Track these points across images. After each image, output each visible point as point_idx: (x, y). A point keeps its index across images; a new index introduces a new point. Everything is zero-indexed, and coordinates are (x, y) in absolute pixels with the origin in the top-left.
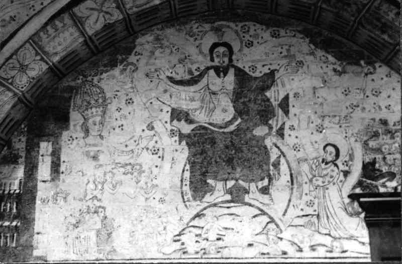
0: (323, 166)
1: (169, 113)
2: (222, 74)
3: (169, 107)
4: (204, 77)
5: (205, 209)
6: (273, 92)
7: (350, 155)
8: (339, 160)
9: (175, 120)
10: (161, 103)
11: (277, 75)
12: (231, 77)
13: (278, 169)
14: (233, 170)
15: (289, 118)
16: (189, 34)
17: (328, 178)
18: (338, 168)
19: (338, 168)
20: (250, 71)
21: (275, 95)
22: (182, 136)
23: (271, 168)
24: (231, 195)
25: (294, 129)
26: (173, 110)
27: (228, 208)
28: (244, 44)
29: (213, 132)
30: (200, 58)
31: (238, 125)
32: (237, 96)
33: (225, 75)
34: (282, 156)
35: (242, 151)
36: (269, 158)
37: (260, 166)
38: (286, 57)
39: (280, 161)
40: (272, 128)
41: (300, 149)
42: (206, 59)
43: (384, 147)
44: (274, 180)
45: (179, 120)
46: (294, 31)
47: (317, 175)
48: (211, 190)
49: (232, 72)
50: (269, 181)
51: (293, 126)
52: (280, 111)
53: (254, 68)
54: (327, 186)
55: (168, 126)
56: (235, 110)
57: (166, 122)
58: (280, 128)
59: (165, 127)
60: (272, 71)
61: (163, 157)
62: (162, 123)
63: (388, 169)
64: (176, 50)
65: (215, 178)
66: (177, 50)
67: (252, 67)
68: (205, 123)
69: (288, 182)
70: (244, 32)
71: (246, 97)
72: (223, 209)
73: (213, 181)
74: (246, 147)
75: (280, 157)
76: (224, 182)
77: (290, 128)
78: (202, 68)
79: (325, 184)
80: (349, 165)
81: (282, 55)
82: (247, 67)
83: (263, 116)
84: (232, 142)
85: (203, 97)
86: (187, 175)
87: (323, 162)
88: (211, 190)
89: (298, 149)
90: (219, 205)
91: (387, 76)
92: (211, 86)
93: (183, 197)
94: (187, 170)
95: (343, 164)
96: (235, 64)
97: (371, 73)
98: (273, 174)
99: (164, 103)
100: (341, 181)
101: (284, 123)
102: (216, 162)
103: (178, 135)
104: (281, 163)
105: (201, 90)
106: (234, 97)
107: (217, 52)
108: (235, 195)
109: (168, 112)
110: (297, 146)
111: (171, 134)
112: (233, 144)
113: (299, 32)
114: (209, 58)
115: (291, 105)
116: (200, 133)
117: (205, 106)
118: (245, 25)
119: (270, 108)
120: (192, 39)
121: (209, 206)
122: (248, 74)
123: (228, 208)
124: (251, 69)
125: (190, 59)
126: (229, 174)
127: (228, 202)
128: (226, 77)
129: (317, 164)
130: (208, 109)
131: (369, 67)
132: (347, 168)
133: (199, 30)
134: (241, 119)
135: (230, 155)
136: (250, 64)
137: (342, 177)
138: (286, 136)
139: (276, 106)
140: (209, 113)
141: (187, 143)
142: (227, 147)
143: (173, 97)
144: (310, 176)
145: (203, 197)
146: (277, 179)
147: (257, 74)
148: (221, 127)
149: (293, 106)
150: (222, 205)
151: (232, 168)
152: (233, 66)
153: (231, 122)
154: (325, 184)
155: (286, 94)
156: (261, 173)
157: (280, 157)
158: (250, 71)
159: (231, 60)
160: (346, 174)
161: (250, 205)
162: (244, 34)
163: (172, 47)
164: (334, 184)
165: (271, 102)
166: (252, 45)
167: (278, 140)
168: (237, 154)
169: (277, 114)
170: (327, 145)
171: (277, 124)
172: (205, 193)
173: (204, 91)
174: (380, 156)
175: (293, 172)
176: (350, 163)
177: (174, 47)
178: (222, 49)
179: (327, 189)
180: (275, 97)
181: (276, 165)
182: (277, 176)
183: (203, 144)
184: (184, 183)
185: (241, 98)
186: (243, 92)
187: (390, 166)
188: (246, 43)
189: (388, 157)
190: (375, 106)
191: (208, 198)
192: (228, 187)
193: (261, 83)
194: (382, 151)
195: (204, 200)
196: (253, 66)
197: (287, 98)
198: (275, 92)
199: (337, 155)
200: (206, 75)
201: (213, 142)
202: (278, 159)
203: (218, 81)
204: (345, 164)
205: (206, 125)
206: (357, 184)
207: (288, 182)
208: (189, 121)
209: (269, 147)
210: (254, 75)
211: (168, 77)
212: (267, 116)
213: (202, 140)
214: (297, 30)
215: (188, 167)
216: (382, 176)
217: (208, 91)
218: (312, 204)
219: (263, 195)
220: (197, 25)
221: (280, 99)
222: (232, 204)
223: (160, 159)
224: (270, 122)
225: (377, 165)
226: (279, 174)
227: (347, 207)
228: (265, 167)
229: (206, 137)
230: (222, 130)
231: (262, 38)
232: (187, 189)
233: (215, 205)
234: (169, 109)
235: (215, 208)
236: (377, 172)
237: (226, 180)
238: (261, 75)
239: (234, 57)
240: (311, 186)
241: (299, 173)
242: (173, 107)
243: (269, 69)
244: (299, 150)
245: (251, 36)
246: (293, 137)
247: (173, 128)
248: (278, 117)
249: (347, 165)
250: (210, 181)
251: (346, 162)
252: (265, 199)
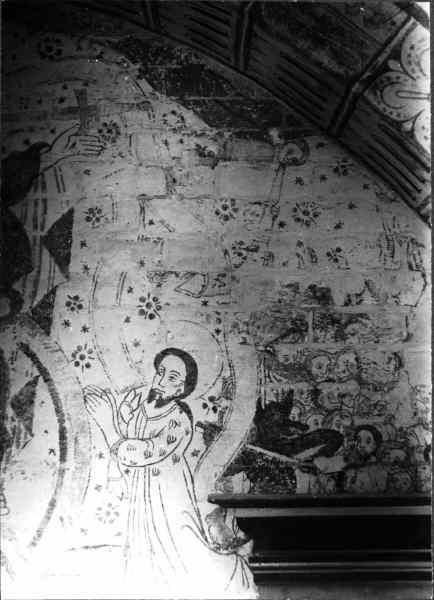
0: (151, 409)
7: (225, 382)
8: (194, 394)
15: (67, 277)
17: (161, 444)
18: (191, 418)
19: (191, 418)
43: (315, 362)
47: (131, 435)
51: (76, 298)
54: (156, 466)
58: (43, 302)
63: (323, 424)
79: (151, 460)
80: (219, 409)
87: (150, 399)
89: (87, 361)
91: (336, 170)
95: (205, 406)
97: (295, 162)
98: (14, 430)
100: (195, 454)
110: (84, 352)
115: (76, 241)
129: (134, 405)
131: (290, 146)
132: (213, 418)
137: (198, 443)
144: (114, 438)
149: (83, 244)
154: (151, 460)
157: (34, 383)
160: (211, 432)
164: (176, 460)
170: (165, 353)
171: (34, 294)
174: (304, 386)
176: (225, 403)
179: (157, 473)
182: (22, 436)
187: (330, 412)
189: (326, 389)
190: (300, 251)
194: (309, 373)
199: (191, 382)
202: (31, 389)
204: (211, 405)
206: (237, 461)
216: (306, 442)
218: (112, 516)
224: (17, 286)
225: (295, 412)
227: (206, 528)
236: (292, 429)
240: (113, 465)
241: (84, 428)
244: (88, 366)
249: (215, 409)
251: (212, 399)
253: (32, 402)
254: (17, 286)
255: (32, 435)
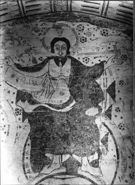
1: (15, 94)
2: (60, 64)
3: (16, 90)
4: (46, 64)
5: (43, 180)
6: (102, 80)
9: (20, 101)
10: (9, 86)
11: (106, 66)
12: (68, 66)
13: (106, 145)
14: (68, 145)
15: (115, 102)
16: (35, 30)
20: (84, 62)
21: (104, 82)
22: (25, 115)
23: (101, 144)
24: (66, 168)
25: (120, 111)
26: (18, 91)
27: (63, 179)
28: (79, 39)
29: (51, 111)
30: (43, 50)
31: (73, 106)
32: (73, 83)
33: (63, 65)
34: (109, 133)
35: (76, 129)
36: (98, 135)
37: (91, 143)
38: (112, 51)
39: (107, 138)
40: (102, 109)
41: (125, 128)
42: (48, 51)
44: (103, 155)
45: (23, 101)
46: (119, 31)
48: (49, 163)
49: (69, 61)
50: (99, 155)
51: (118, 108)
52: (108, 95)
53: (87, 60)
55: (14, 106)
56: (71, 94)
57: (12, 102)
58: (108, 109)
59: (11, 106)
60: (102, 62)
61: (8, 133)
62: (8, 103)
64: (23, 42)
65: (53, 152)
66: (24, 43)
67: (86, 59)
68: (46, 104)
69: (115, 156)
70: (79, 30)
71: (79, 83)
72: (58, 180)
73: (51, 155)
74: (80, 125)
75: (107, 134)
76: (60, 156)
77: (116, 110)
78: (45, 58)
81: (110, 49)
82: (81, 58)
83: (93, 99)
84: (67, 120)
85: (45, 81)
86: (28, 148)
88: (49, 163)
90: (55, 177)
92: (51, 73)
93: (24, 168)
94: (29, 145)
96: (72, 56)
98: (102, 149)
99: (11, 86)
101: (111, 106)
102: (54, 138)
103: (22, 113)
104: (109, 140)
105: (43, 75)
106: (70, 83)
107: (57, 45)
108: (69, 168)
109: (14, 93)
111: (16, 112)
112: (69, 123)
113: (123, 32)
114: (50, 50)
116: (41, 113)
117: (46, 89)
118: (81, 25)
119: (100, 92)
120: (37, 34)
121: (47, 178)
122: (83, 64)
123: (63, 179)
124: (85, 60)
125: (34, 50)
126: (65, 148)
127: (63, 174)
128: (64, 66)
130: (48, 91)
133: (42, 27)
134: (76, 101)
135: (65, 132)
136: (84, 56)
138: (113, 117)
139: (104, 91)
140: (49, 95)
141: (29, 121)
142: (63, 125)
143: (19, 81)
145: (42, 169)
146: (105, 154)
147: (89, 65)
148: (59, 108)
150: (58, 177)
151: (67, 143)
152: (70, 57)
153: (67, 104)
155: (113, 81)
156: (92, 148)
157: (107, 134)
158: (84, 62)
159: (68, 52)
161: (82, 177)
162: (80, 32)
163: (20, 40)
165: (101, 88)
166: (86, 41)
167: (106, 120)
168: (72, 131)
169: (105, 98)
171: (106, 107)
172: (44, 166)
173: (45, 77)
175: (118, 148)
177: (21, 39)
178: (61, 43)
180: (104, 84)
181: (105, 141)
182: (105, 151)
183: (43, 121)
184: (26, 157)
185: (76, 83)
186: (77, 78)
188: (81, 39)
191: (46, 171)
192: (63, 161)
193: (93, 72)
195: (42, 172)
196: (86, 57)
197: (113, 84)
198: (104, 80)
200: (48, 64)
201: (51, 120)
203: (58, 69)
205: (47, 106)
207: (115, 156)
208: (31, 102)
209: (98, 126)
210: (87, 65)
211: (15, 64)
212: (97, 99)
213: (42, 119)
214: (122, 30)
215: (29, 142)
217: (48, 77)
219: (93, 168)
220: (42, 23)
221: (108, 86)
222: (67, 176)
223: (6, 134)
224: (100, 104)
226: (107, 149)
228: (95, 143)
229: (46, 116)
230: (60, 110)
231: (94, 35)
232: (27, 161)
233: (52, 177)
234: (16, 91)
235: (52, 180)
237: (62, 154)
238: (93, 65)
239: (70, 50)
242: (19, 89)
243: (100, 60)
245: (85, 34)
246: (119, 117)
247: (18, 107)
248: (106, 100)
250: (47, 155)
252: (95, 171)
253: (107, 141)
254: (100, 104)
255: (108, 151)
